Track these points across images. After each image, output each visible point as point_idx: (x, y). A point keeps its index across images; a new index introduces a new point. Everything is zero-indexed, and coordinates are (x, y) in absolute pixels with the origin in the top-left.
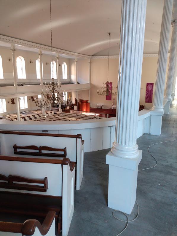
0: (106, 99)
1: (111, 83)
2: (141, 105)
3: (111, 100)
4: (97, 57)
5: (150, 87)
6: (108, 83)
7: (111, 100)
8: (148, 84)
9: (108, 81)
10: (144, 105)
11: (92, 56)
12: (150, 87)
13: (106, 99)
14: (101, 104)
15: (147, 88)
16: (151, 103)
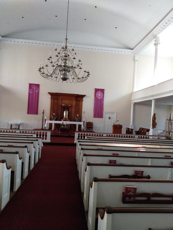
0: (28, 113)
1: (38, 86)
2: (88, 122)
3: (37, 114)
4: (13, 40)
5: (99, 95)
6: (31, 85)
7: (37, 114)
8: (97, 90)
9: (66, 46)
10: (91, 122)
11: (2, 37)
12: (99, 94)
13: (28, 113)
14: (19, 122)
15: (95, 96)
16: (102, 118)
